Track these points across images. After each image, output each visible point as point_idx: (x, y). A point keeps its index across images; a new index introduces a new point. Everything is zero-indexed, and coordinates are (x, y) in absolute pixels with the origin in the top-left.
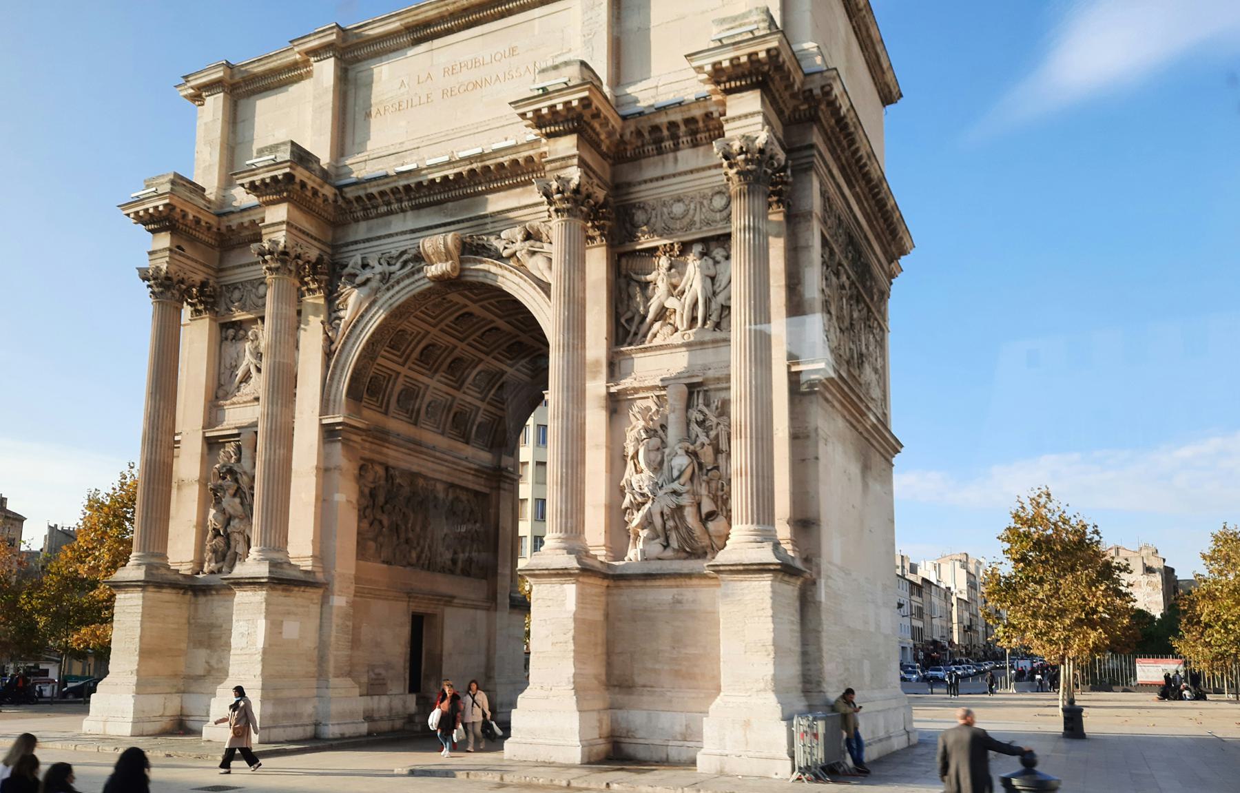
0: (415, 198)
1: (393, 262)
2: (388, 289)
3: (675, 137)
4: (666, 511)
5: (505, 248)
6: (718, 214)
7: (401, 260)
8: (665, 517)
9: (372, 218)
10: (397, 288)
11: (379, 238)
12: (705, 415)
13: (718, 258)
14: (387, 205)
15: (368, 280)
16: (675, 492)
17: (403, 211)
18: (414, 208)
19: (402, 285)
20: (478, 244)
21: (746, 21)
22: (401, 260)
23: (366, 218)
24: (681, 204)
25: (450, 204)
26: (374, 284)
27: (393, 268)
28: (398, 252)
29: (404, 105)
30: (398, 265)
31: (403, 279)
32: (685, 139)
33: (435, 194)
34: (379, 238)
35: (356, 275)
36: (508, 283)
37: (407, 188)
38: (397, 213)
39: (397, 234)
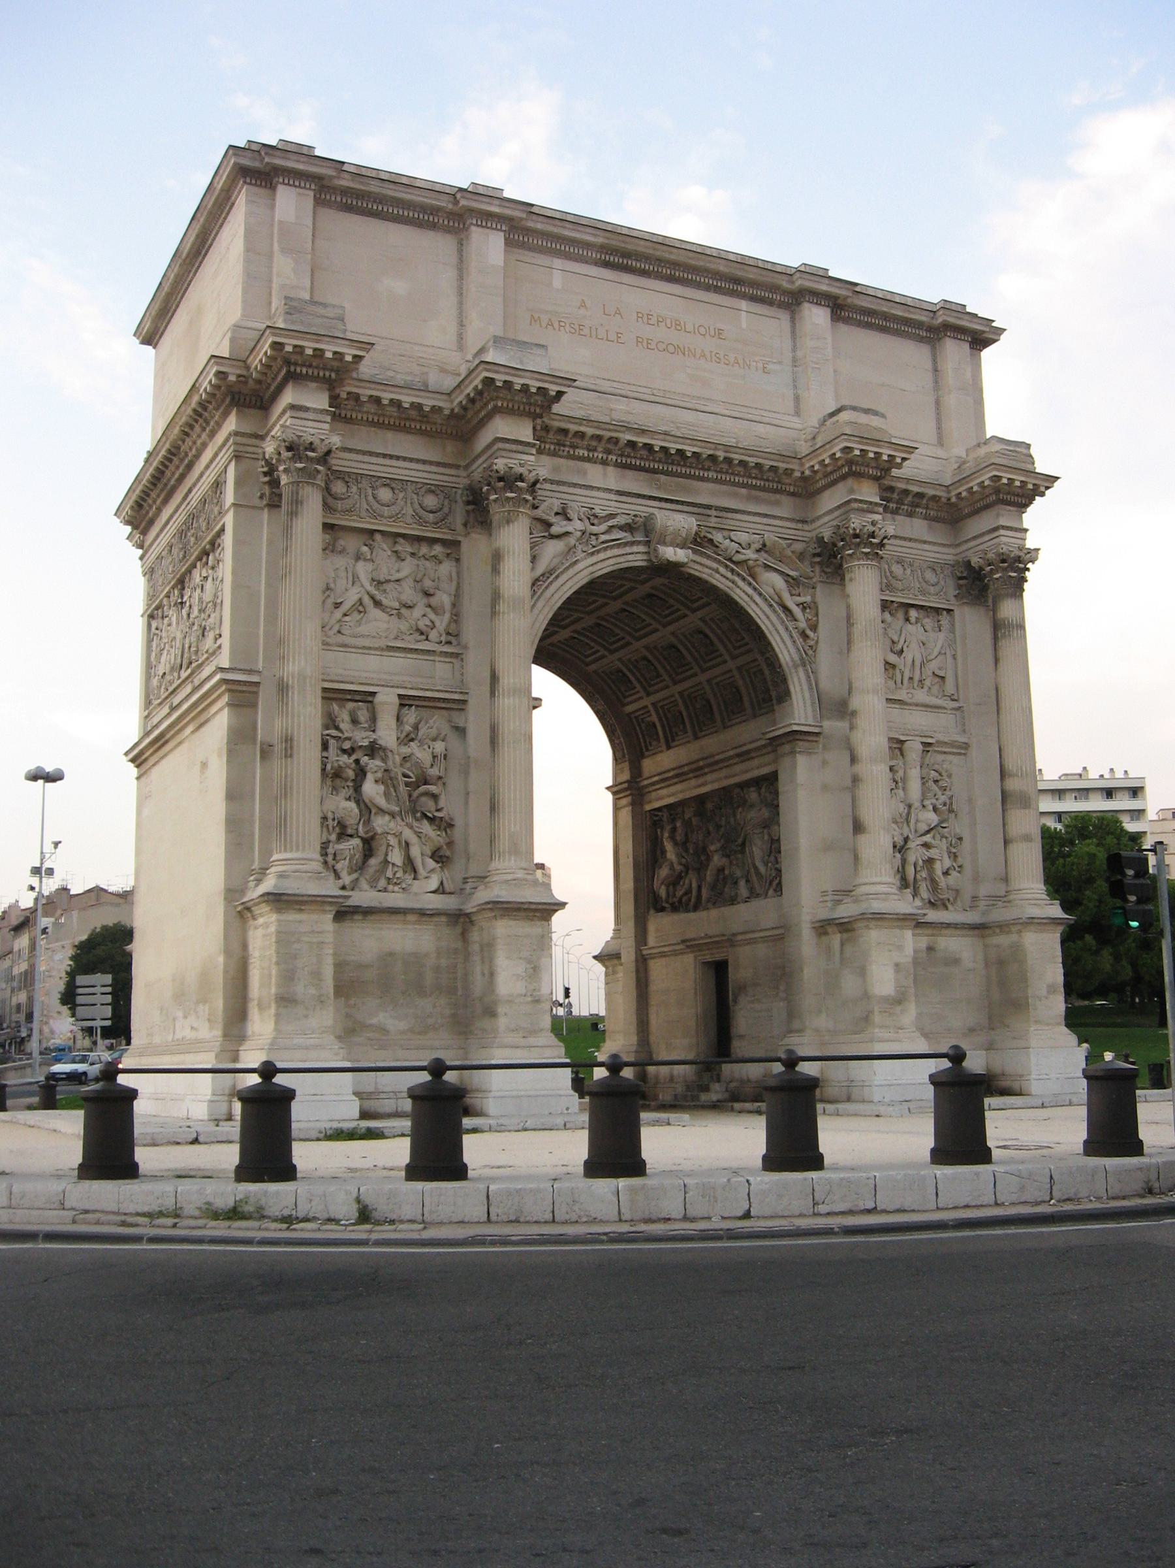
0: (628, 456)
1: (596, 521)
2: (592, 554)
3: (900, 502)
4: (920, 862)
5: (737, 552)
6: (932, 588)
7: (610, 523)
8: (918, 869)
9: (561, 457)
10: (602, 556)
11: (575, 485)
12: (940, 775)
13: (927, 628)
14: (589, 450)
15: (567, 534)
16: (926, 845)
17: (604, 463)
18: (617, 465)
19: (609, 553)
20: (705, 537)
21: (1018, 449)
22: (610, 523)
23: (554, 454)
24: (899, 566)
25: (663, 478)
26: (572, 541)
27: (595, 529)
28: (605, 513)
29: (586, 331)
30: (603, 527)
31: (612, 547)
32: (906, 507)
33: (654, 460)
34: (575, 485)
35: (549, 525)
36: (738, 591)
37: (632, 444)
38: (595, 463)
39: (599, 489)
